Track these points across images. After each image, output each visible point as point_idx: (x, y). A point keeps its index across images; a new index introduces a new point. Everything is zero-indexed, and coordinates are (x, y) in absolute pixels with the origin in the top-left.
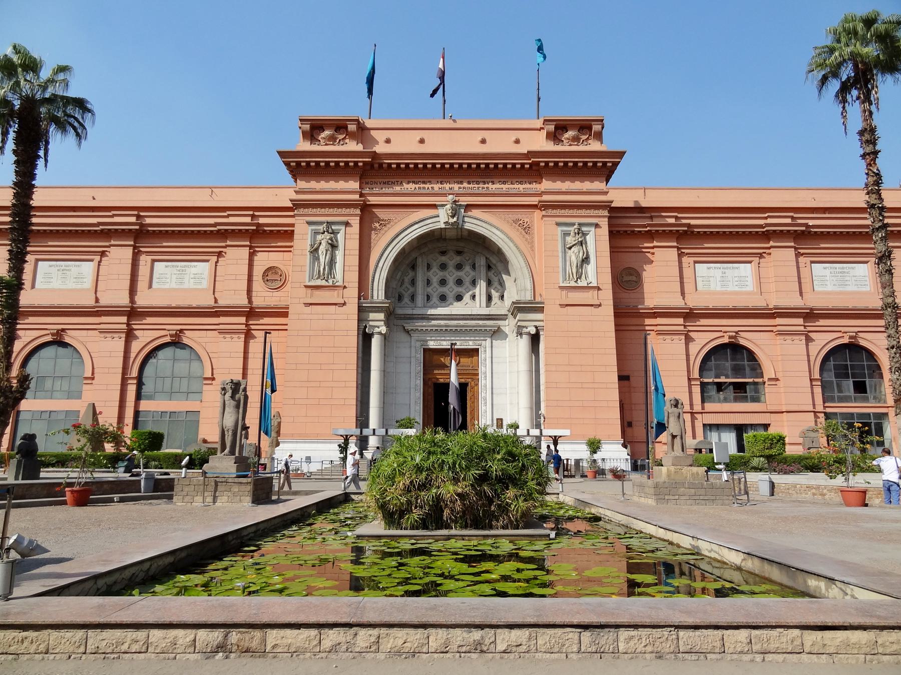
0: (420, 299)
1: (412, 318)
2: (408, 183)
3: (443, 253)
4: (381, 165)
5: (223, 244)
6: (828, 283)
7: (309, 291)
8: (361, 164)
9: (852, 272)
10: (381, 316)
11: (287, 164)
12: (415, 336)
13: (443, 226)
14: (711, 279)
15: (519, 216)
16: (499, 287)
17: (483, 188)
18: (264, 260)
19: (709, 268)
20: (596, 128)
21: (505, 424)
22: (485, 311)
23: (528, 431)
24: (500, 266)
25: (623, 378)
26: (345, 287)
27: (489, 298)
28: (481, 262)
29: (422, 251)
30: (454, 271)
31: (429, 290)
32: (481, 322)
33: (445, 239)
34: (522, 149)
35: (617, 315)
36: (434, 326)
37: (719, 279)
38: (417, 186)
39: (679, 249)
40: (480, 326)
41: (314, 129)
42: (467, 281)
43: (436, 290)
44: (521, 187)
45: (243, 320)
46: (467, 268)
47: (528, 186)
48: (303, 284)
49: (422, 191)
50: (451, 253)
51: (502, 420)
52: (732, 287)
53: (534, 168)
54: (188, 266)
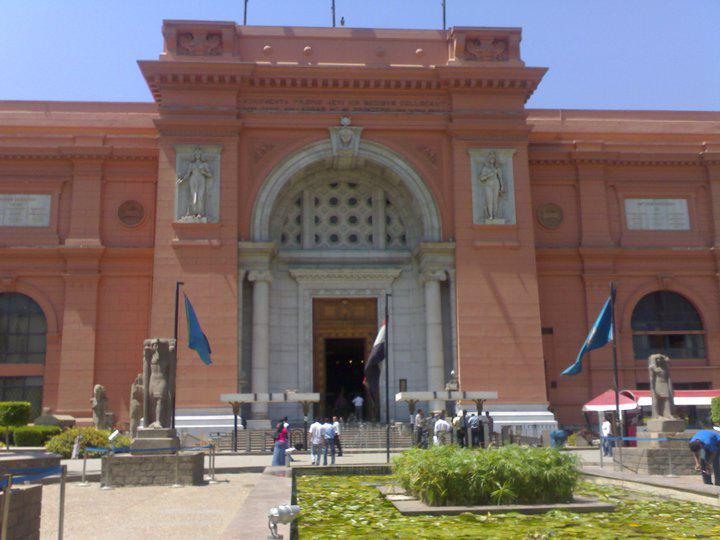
0: (308, 241)
3: (334, 185)
10: (266, 259)
12: (303, 282)
13: (336, 154)
14: (644, 217)
16: (399, 226)
19: (640, 204)
20: (513, 39)
21: (409, 384)
22: (383, 255)
25: (547, 331)
26: (222, 226)
27: (389, 239)
28: (379, 196)
31: (318, 229)
33: (336, 170)
41: (179, 34)
42: (362, 219)
46: (362, 203)
50: (343, 186)
51: (405, 381)
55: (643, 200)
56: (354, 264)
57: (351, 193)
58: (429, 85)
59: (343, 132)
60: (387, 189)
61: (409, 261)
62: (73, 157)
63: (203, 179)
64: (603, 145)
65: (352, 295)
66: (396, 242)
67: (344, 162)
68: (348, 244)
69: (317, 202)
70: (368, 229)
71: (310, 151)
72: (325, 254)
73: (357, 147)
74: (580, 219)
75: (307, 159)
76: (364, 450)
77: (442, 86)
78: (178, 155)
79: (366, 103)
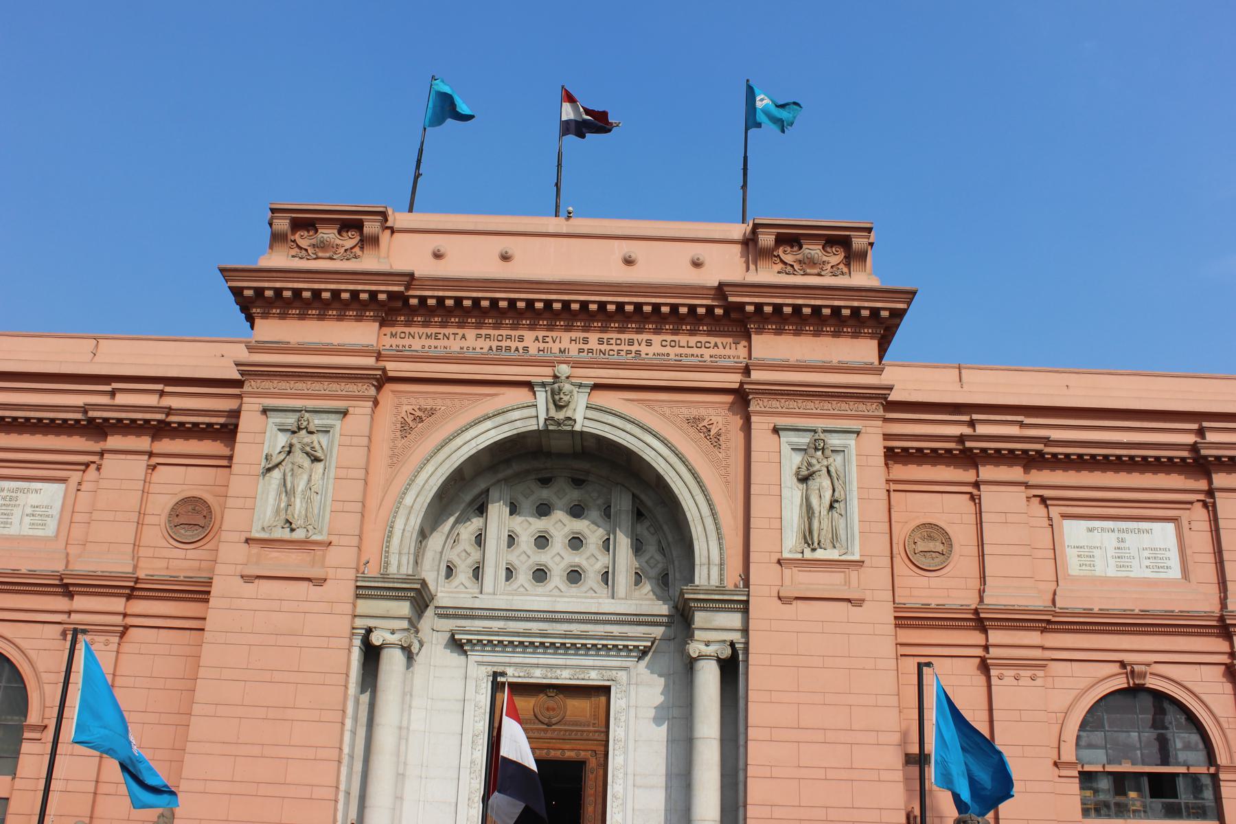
1: (469, 614)
2: (479, 336)
3: (545, 482)
4: (423, 300)
5: (97, 447)
7: (255, 549)
8: (382, 297)
10: (404, 608)
11: (237, 292)
14: (1097, 553)
15: (702, 412)
16: (658, 557)
18: (178, 481)
19: (1090, 530)
27: (638, 578)
28: (622, 503)
29: (500, 476)
31: (513, 557)
32: (616, 630)
33: (549, 454)
34: (710, 277)
36: (518, 634)
37: (1111, 552)
38: (495, 344)
39: (1027, 486)
40: (614, 638)
43: (526, 557)
44: (707, 353)
45: (118, 604)
47: (721, 351)
48: (244, 536)
49: (504, 355)
52: (1139, 571)
53: (733, 315)
54: (23, 491)
57: (574, 495)
58: (710, 309)
60: (637, 492)
62: (106, 420)
63: (306, 462)
64: (1021, 425)
70: (603, 560)
71: (499, 420)
74: (982, 556)
75: (493, 433)
77: (730, 315)
78: (271, 420)
79: (601, 341)
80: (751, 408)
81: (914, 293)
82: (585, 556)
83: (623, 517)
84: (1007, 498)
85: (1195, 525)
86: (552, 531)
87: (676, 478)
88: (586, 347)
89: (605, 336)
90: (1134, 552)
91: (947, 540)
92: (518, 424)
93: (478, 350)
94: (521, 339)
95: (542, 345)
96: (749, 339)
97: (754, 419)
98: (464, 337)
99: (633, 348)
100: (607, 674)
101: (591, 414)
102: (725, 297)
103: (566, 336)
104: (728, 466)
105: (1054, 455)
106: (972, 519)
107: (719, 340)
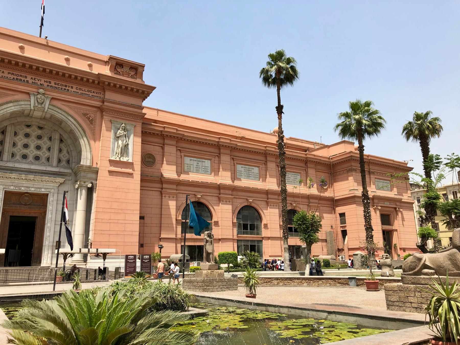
2: (9, 73)
3: (28, 126)
6: (243, 175)
9: (253, 171)
13: (32, 108)
14: (192, 166)
15: (88, 112)
16: (67, 155)
17: (65, 89)
19: (191, 160)
20: (140, 69)
23: (80, 249)
24: (69, 141)
25: (142, 218)
27: (59, 161)
28: (56, 137)
30: (35, 140)
31: (15, 150)
35: (142, 180)
37: (195, 166)
38: (15, 77)
42: (44, 148)
43: (19, 150)
44: (91, 94)
53: (101, 84)
55: (192, 159)
56: (36, 173)
57: (39, 132)
58: (93, 81)
59: (39, 96)
60: (62, 134)
61: (70, 175)
64: (177, 130)
65: (32, 190)
66: (64, 163)
67: (38, 114)
68: (33, 161)
69: (16, 134)
70: (47, 154)
72: (17, 165)
73: (46, 109)
75: (13, 108)
76: (31, 283)
77: (99, 83)
79: (55, 84)
80: (104, 113)
81: (154, 88)
82: (42, 152)
83: (56, 141)
84: (170, 150)
85: (216, 162)
86: (30, 142)
87: (78, 131)
88: (50, 85)
89: (57, 82)
90: (200, 167)
91: (154, 158)
92: (23, 106)
93: (9, 78)
94: (26, 77)
95: (34, 81)
96: (105, 92)
97: (104, 117)
98: (3, 72)
99: (67, 88)
100: (48, 190)
101: (50, 107)
102: (99, 78)
103: (43, 80)
104: (95, 130)
105: (185, 139)
106: (161, 153)
107: (95, 91)
